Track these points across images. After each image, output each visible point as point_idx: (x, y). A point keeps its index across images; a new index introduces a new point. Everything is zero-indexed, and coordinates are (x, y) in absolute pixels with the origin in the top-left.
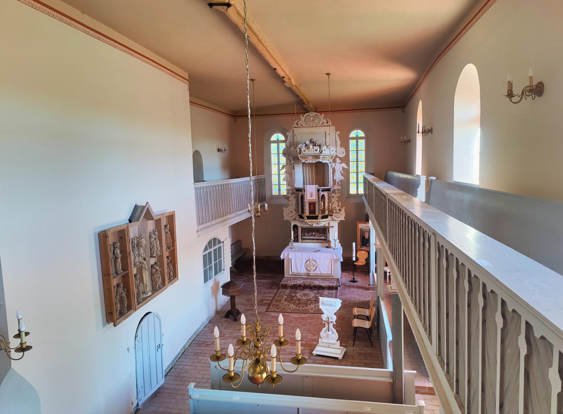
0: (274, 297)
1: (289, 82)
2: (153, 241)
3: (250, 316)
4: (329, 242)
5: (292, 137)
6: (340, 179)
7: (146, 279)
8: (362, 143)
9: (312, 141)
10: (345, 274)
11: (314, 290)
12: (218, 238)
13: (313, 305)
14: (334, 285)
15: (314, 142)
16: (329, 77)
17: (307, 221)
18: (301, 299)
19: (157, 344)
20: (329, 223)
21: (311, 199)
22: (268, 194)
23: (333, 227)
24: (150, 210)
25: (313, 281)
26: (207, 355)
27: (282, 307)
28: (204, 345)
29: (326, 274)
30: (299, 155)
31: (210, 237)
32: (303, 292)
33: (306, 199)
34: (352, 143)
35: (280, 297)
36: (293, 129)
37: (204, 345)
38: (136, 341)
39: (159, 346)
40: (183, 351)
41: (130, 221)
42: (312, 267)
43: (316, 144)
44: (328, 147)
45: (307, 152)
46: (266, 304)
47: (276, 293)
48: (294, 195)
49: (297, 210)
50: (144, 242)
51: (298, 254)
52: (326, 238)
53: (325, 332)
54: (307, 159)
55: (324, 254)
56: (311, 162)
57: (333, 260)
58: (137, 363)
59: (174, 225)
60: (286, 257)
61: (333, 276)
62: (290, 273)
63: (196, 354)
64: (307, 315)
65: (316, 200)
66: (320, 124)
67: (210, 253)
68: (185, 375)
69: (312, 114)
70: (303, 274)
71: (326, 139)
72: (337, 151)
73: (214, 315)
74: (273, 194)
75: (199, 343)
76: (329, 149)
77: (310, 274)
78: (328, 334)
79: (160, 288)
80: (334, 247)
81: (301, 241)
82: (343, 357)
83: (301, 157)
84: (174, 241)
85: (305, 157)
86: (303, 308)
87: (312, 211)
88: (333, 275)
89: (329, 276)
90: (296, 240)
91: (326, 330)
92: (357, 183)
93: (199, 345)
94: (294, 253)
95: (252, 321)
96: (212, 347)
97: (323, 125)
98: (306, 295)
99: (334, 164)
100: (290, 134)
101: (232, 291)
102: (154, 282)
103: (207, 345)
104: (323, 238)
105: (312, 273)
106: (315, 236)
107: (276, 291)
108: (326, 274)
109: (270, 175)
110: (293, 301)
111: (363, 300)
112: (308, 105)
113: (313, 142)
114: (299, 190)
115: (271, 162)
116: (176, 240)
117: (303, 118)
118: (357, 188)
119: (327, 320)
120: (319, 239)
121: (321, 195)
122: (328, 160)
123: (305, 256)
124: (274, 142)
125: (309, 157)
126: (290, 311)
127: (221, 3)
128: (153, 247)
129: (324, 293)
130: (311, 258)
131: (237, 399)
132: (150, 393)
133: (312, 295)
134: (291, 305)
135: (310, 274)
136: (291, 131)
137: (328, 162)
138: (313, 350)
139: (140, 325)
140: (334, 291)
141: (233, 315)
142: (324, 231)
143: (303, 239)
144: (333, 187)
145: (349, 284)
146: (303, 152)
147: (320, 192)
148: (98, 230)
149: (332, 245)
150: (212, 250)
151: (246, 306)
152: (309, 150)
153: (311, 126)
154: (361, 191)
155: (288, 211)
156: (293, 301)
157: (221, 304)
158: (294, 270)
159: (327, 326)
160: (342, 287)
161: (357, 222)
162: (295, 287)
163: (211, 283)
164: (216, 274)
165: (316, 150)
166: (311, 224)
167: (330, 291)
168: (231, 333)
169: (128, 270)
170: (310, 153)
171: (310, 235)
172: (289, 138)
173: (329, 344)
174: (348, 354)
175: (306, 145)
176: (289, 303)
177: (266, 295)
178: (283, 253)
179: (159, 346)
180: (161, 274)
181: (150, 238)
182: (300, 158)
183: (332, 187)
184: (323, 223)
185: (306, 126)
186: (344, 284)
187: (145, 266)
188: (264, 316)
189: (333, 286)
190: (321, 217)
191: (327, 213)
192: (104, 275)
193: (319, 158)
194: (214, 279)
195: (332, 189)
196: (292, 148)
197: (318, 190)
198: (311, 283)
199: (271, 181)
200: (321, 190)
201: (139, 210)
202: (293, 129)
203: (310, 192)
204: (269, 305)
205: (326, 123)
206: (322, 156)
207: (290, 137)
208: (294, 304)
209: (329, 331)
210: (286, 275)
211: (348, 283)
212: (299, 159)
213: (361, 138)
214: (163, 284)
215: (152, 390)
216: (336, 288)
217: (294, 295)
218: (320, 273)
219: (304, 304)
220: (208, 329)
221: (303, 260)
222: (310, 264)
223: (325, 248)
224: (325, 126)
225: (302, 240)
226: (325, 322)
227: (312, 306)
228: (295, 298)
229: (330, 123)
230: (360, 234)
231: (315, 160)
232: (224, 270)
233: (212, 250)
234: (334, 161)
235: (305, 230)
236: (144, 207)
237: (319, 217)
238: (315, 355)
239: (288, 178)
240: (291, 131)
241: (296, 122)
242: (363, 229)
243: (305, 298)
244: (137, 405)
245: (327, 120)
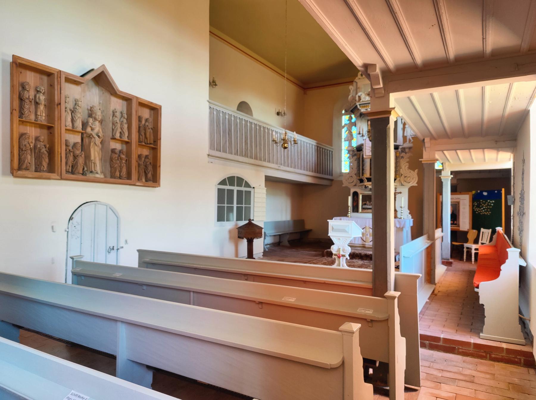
12: (245, 179)
22: (335, 170)
23: (400, 193)
30: (358, 104)
59: (159, 121)
81: (362, 211)
90: (355, 209)
116: (160, 139)
128: (115, 128)
135: (366, 246)
146: (362, 99)
172: (351, 91)
181: (113, 117)
182: (359, 107)
195: (401, 147)
222: (367, 233)
225: (363, 210)
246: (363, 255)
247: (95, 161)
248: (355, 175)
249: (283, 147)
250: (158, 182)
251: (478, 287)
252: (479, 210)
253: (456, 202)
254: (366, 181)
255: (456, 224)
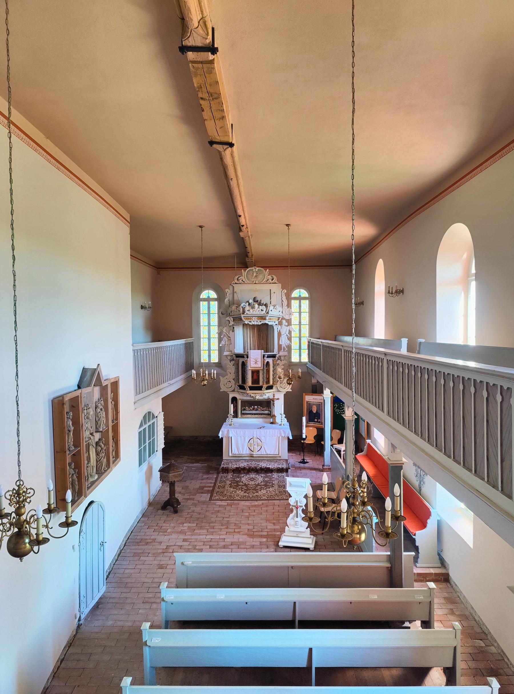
0: (215, 483)
1: (246, 231)
2: (100, 412)
3: (191, 506)
4: (274, 416)
5: (231, 295)
6: (285, 343)
7: (93, 458)
8: (305, 304)
9: (257, 299)
10: (291, 454)
11: (261, 473)
12: (152, 412)
13: (265, 491)
14: (284, 466)
15: (258, 301)
16: (288, 228)
17: (249, 392)
18: (249, 484)
19: (100, 542)
20: (274, 395)
21: (255, 366)
22: (196, 361)
23: (278, 399)
24: (101, 375)
25: (259, 463)
26: (150, 555)
27: (228, 494)
28: (144, 544)
29: (272, 455)
30: (242, 316)
31: (145, 411)
32: (248, 476)
33: (249, 367)
34: (295, 304)
35: (223, 482)
36: (234, 285)
37: (144, 544)
38: (81, 537)
39: (102, 543)
40: (119, 552)
41: (79, 387)
42: (256, 446)
43: (260, 303)
44: (275, 307)
45: (251, 312)
46: (208, 492)
47: (216, 479)
48: (233, 362)
49: (236, 380)
50: (92, 413)
51: (240, 431)
52: (270, 413)
53: (293, 518)
54: (251, 320)
55: (271, 430)
56: (256, 323)
57: (280, 437)
58: (81, 565)
60: (225, 435)
61: (280, 457)
62: (230, 455)
63: (136, 554)
64: (260, 502)
65: (261, 367)
66: (264, 281)
67: (145, 429)
68: (129, 580)
69: (255, 268)
70: (245, 455)
71: (271, 299)
72: (283, 312)
73: (147, 507)
74: (202, 361)
75: (137, 541)
76: (276, 309)
77: (253, 455)
78: (296, 521)
79: (105, 471)
80: (280, 423)
81: (241, 416)
82: (315, 548)
83: (245, 317)
84: (118, 413)
85: (249, 317)
86: (254, 495)
87: (255, 380)
88: (280, 455)
89: (275, 457)
90: (236, 416)
91: (294, 516)
92: (300, 349)
93: (138, 543)
94: (235, 430)
95: (196, 513)
96: (155, 545)
97: (267, 282)
98: (252, 479)
99: (279, 327)
100: (229, 291)
101: (173, 476)
102: (98, 463)
103: (147, 544)
104: (266, 412)
105: (255, 454)
106: (257, 410)
107: (216, 476)
108: (272, 455)
109: (199, 339)
110: (239, 487)
111: (319, 482)
112: (251, 258)
113: (257, 301)
114: (239, 356)
115: (200, 323)
117: (244, 273)
118: (300, 355)
119: (296, 504)
120: (262, 414)
121: (266, 362)
122: (275, 322)
123: (248, 433)
124: (204, 300)
125: (254, 318)
126: (238, 498)
127: (223, 142)
128: (99, 420)
129: (273, 476)
130: (255, 436)
131: (222, 597)
132: (92, 604)
133: (260, 479)
134: (237, 491)
135: (254, 455)
136: (231, 287)
137: (274, 324)
138: (279, 542)
139: (85, 516)
140: (284, 474)
141: (172, 506)
142: (268, 404)
143: (243, 414)
144: (279, 354)
145: (299, 466)
146: (247, 312)
147: (265, 358)
148: (52, 397)
149: (278, 420)
150: (146, 426)
151: (184, 495)
152: (254, 309)
153: (254, 282)
154: (305, 358)
155: (226, 381)
156: (239, 487)
157: (154, 494)
158: (235, 451)
159: (295, 512)
160: (291, 469)
161: (304, 394)
162: (238, 471)
163: (145, 466)
164: (150, 456)
165: (262, 310)
166: (253, 396)
167: (280, 474)
168: (174, 527)
169: (80, 447)
170: (255, 313)
171: (252, 409)
172: (228, 295)
173: (297, 533)
174: (319, 543)
175: (249, 304)
176: (235, 490)
177: (205, 481)
178: (222, 430)
179: (102, 544)
180: (106, 453)
181: (96, 408)
182: (243, 319)
183: (277, 353)
184: (267, 394)
185: (249, 282)
186: (293, 466)
187: (92, 443)
188: (209, 506)
189: (283, 468)
190: (266, 387)
191: (271, 383)
192: (57, 452)
193: (265, 319)
194: (148, 462)
195: (277, 356)
196: (234, 307)
197: (264, 356)
198: (256, 465)
199: (199, 346)
200: (266, 356)
201: (89, 374)
202: (234, 285)
203: (254, 358)
204: (212, 492)
205: (271, 280)
206: (268, 317)
207: (229, 294)
208: (242, 491)
209: (297, 517)
210: (225, 457)
211: (298, 465)
212: (242, 320)
213: (305, 298)
214: (108, 466)
215: (94, 600)
216: (286, 470)
217: (239, 480)
218: (265, 453)
219: (253, 490)
220: (144, 524)
221: (246, 438)
222: (254, 443)
223: (269, 424)
224: (270, 283)
225: (243, 415)
226: (293, 507)
227: (264, 492)
228: (241, 483)
229: (275, 280)
230: (307, 409)
231: (260, 322)
232: (157, 451)
233: (146, 426)
234: (280, 323)
235: (245, 403)
236: (95, 370)
237: (264, 387)
238: (282, 547)
239: (227, 342)
240: (231, 287)
241: (237, 277)
242: (310, 402)
243: (253, 483)
244: (79, 620)
245: (272, 276)
246: (259, 468)
247: (93, 464)
248: (233, 380)
249: (203, 384)
250: (119, 456)
251: (415, 535)
252: (339, 411)
253: (320, 402)
254: (249, 390)
255: (320, 422)
